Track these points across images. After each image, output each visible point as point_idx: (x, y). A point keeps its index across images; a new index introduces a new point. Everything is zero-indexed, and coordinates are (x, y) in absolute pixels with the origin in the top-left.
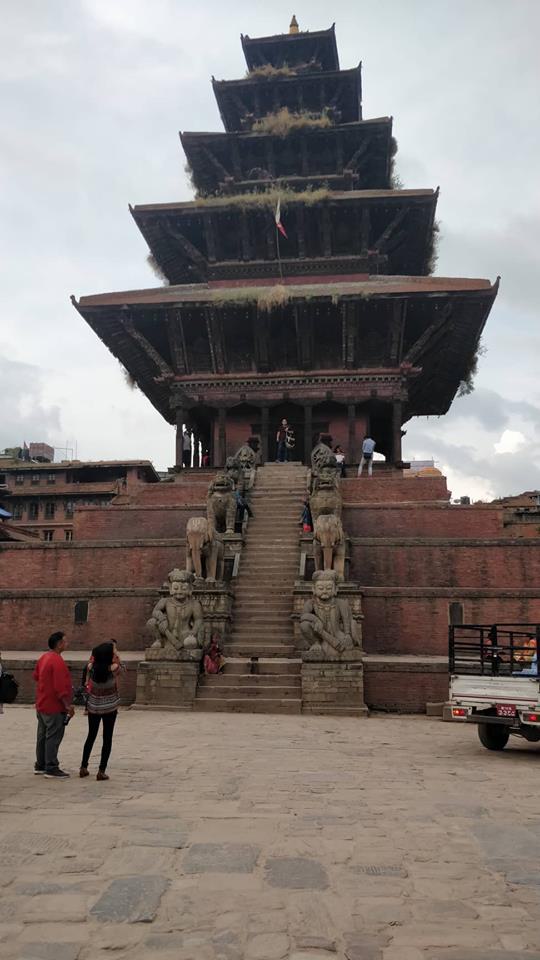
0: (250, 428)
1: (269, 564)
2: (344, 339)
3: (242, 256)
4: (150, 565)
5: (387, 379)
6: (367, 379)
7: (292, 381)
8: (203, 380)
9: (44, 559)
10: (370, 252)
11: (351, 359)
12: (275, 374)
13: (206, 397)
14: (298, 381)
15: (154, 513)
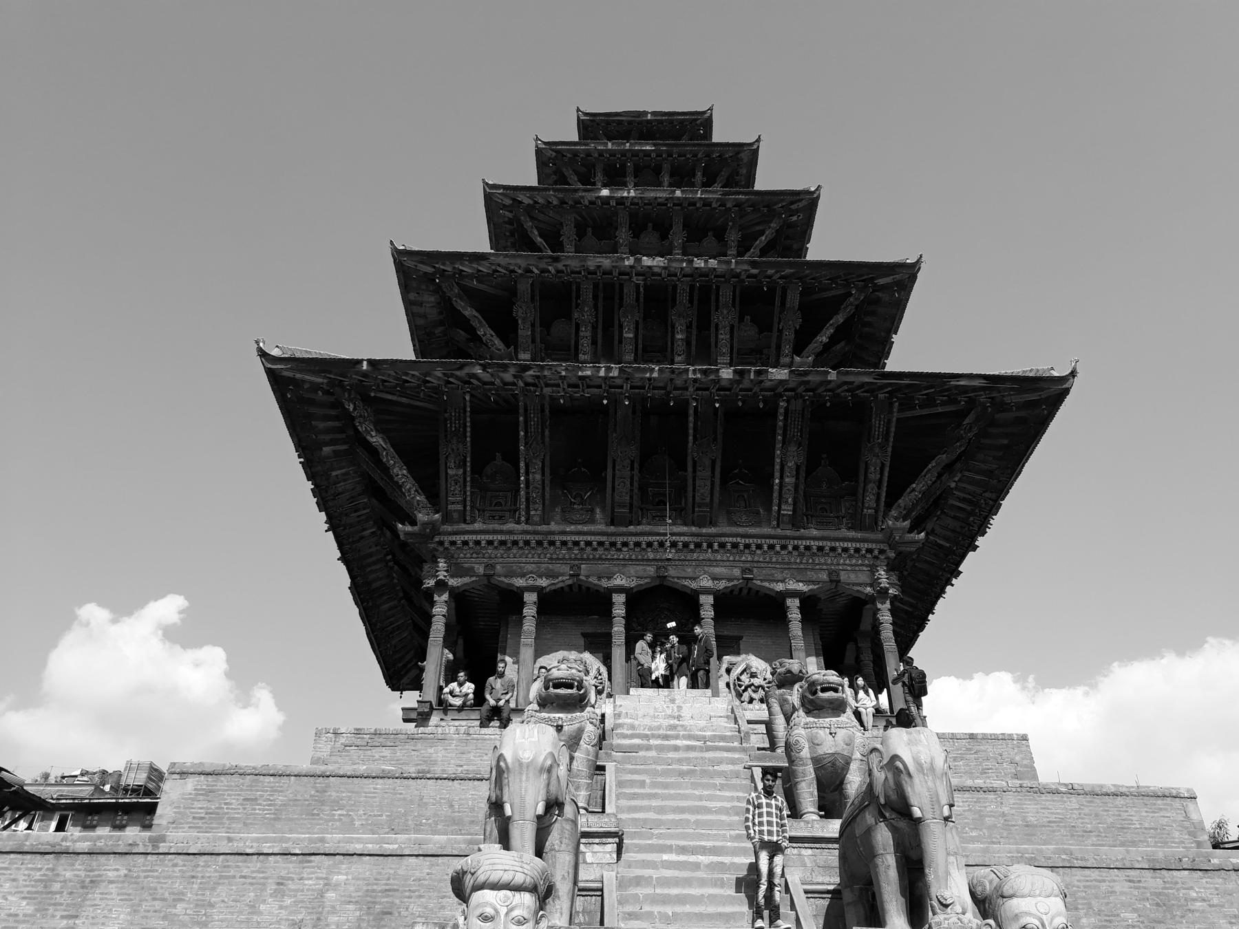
0: (582, 642)
1: (698, 900)
2: (777, 467)
3: (577, 355)
4: (351, 907)
5: (857, 550)
6: (820, 549)
7: (674, 544)
8: (495, 532)
9: (46, 882)
10: (797, 359)
11: (787, 510)
12: (640, 528)
13: (498, 567)
14: (686, 545)
15: (369, 785)
